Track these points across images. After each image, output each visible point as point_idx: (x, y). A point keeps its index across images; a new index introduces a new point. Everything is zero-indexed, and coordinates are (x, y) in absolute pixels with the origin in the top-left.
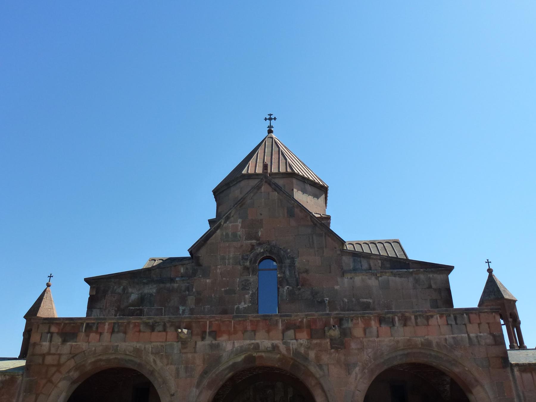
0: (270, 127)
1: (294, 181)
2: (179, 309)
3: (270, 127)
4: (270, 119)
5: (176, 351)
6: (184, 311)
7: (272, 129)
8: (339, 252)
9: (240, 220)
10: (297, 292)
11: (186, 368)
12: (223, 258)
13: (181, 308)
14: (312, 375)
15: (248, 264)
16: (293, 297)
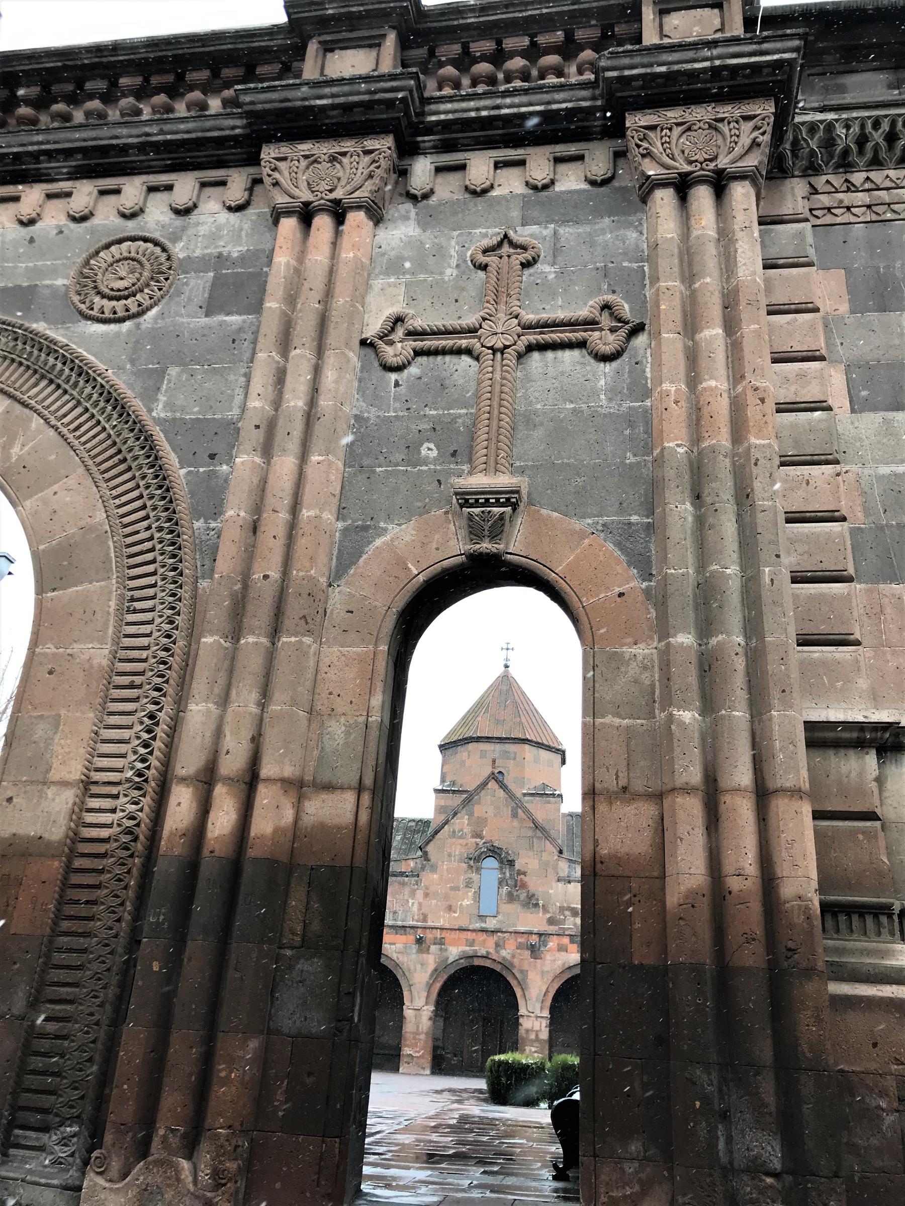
0: (507, 660)
1: (527, 747)
2: (408, 902)
3: (507, 660)
4: (508, 649)
5: (414, 951)
6: (413, 903)
7: (509, 663)
8: (556, 857)
9: (466, 817)
10: (515, 894)
11: (422, 965)
12: (450, 855)
13: (411, 901)
14: (516, 978)
15: (472, 862)
16: (511, 898)
